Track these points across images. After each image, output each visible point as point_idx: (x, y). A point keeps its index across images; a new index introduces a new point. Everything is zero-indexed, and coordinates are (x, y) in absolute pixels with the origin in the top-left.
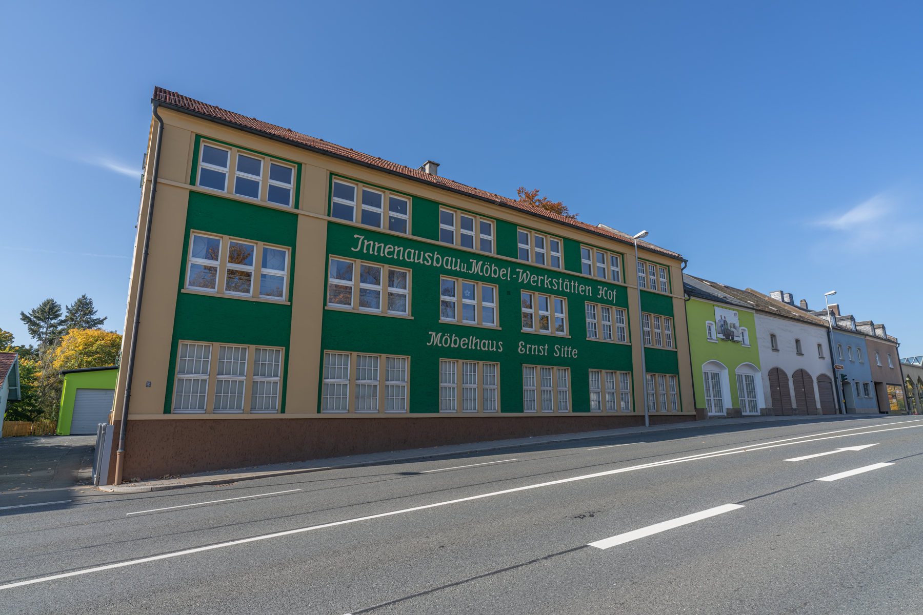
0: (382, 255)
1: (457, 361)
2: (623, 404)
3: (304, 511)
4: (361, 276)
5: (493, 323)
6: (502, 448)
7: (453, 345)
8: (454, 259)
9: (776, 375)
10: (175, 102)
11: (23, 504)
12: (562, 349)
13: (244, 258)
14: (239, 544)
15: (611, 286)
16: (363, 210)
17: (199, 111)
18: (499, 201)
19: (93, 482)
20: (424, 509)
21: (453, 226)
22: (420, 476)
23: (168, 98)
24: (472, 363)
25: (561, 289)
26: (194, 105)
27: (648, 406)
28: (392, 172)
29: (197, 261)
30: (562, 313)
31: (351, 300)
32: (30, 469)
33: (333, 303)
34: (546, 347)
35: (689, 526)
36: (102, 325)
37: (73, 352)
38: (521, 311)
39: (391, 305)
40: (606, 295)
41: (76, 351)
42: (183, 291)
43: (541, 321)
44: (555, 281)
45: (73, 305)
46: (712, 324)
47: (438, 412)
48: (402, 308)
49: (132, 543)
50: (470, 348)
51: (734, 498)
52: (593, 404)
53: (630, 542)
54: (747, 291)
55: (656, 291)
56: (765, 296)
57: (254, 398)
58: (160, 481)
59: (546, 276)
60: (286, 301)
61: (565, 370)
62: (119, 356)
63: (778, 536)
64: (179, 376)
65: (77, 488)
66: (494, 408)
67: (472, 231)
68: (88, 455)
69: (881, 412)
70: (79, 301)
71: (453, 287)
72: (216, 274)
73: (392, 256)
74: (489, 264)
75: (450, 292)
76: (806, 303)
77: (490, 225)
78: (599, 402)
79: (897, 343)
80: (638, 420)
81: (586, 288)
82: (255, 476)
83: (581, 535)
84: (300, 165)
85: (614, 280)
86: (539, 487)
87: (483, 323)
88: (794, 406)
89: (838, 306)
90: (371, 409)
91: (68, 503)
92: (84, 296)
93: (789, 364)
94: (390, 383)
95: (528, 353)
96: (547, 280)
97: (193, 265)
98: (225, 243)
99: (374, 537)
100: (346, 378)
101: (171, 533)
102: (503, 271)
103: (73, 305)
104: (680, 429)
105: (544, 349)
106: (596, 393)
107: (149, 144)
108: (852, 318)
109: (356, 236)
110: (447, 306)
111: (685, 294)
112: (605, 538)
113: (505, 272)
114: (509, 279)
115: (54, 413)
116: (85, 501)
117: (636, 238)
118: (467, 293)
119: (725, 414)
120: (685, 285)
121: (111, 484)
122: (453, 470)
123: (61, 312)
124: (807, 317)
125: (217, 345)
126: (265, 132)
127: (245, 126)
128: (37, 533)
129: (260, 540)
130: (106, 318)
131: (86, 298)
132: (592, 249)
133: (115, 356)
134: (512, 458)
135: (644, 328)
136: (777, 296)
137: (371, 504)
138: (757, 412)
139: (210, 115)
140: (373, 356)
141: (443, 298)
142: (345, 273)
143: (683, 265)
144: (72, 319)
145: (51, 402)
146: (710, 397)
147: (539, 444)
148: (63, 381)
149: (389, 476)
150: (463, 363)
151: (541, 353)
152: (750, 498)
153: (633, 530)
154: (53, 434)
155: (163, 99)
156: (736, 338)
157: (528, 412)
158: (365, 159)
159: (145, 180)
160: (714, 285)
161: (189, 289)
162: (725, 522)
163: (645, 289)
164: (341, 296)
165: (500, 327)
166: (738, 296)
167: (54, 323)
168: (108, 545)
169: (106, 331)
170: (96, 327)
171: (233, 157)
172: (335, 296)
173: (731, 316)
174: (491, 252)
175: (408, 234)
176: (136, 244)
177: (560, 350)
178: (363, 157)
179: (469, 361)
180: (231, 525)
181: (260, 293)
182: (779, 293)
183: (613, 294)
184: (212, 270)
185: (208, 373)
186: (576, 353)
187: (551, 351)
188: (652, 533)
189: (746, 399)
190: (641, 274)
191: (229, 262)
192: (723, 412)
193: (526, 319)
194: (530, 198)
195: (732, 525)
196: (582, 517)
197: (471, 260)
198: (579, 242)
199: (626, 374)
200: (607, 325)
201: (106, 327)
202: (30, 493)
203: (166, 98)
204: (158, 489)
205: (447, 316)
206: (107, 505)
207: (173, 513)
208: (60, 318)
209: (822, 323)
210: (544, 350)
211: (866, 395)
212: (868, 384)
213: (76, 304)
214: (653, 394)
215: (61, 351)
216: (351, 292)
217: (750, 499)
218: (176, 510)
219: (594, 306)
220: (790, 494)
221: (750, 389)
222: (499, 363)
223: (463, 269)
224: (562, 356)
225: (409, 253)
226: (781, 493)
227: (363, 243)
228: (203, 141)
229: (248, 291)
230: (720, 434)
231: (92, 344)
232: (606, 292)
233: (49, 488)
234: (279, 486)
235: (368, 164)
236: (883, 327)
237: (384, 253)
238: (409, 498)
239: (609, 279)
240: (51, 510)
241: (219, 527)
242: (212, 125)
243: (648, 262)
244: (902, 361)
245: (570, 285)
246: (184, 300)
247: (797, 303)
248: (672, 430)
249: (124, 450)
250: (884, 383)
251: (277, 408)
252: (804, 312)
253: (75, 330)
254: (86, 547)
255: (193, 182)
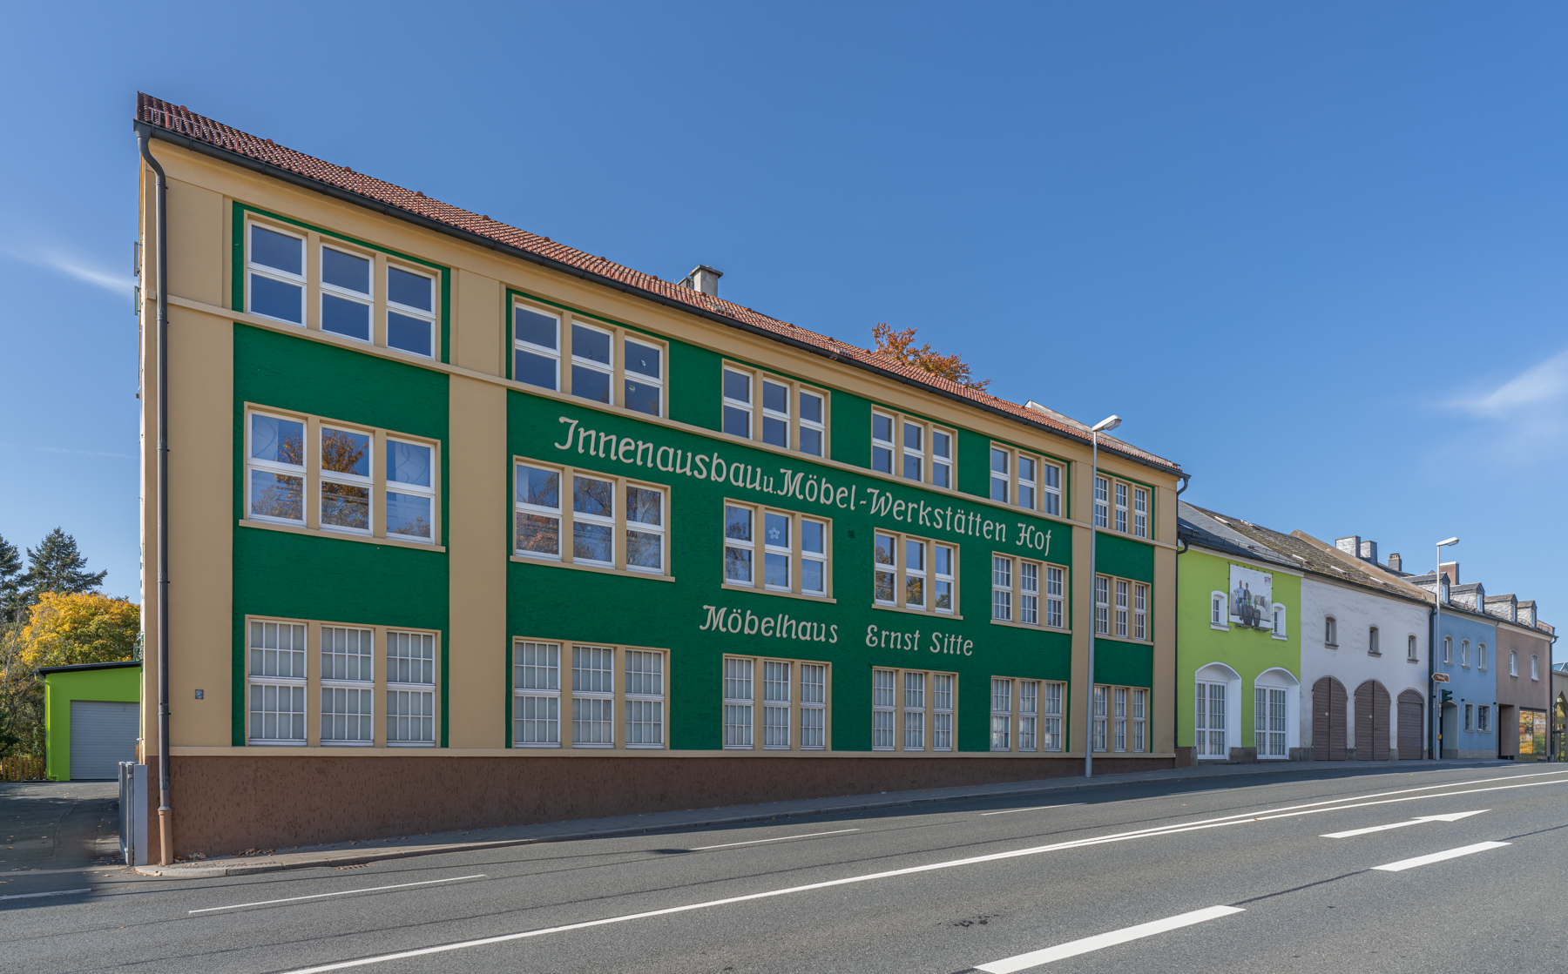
0: (613, 457)
1: (755, 660)
2: (1048, 737)
3: (493, 910)
4: (575, 499)
5: (822, 590)
6: (832, 811)
7: (747, 631)
8: (750, 468)
9: (1327, 692)
10: (184, 128)
11: (8, 895)
12: (946, 640)
13: (351, 462)
14: (387, 961)
15: (1041, 523)
16: (573, 366)
17: (234, 150)
18: (838, 352)
19: (124, 860)
20: (698, 909)
21: (748, 402)
22: (691, 856)
23: (167, 119)
24: (782, 662)
25: (948, 528)
26: (222, 134)
27: (1092, 742)
28: (629, 289)
29: (262, 465)
30: (949, 573)
31: (557, 544)
32: (10, 838)
33: (524, 549)
34: (917, 635)
35: (1148, 941)
36: (99, 586)
37: (54, 635)
38: (873, 569)
39: (632, 555)
40: (1032, 542)
41: (58, 633)
42: (242, 523)
43: (909, 588)
44: (939, 513)
45: (40, 548)
46: (1222, 597)
47: (721, 748)
48: (651, 561)
49: (204, 958)
50: (778, 635)
51: (1229, 896)
52: (995, 738)
53: (1046, 964)
54: (1295, 536)
55: (1125, 535)
56: (1327, 546)
57: (391, 720)
58: (239, 859)
59: (922, 502)
60: (436, 544)
61: (949, 677)
62: (139, 642)
63: (1296, 957)
64: (251, 680)
65: (97, 869)
66: (820, 743)
67: (785, 412)
68: (109, 815)
69: (1501, 757)
70: (49, 539)
71: (747, 522)
72: (301, 491)
73: (632, 460)
74: (815, 477)
75: (742, 532)
76: (1400, 561)
77: (820, 400)
78: (1007, 734)
79: (1552, 636)
80: (1073, 765)
81: (995, 527)
82: (403, 852)
83: (964, 953)
84: (446, 271)
85: (1049, 512)
86: (895, 876)
87: (803, 590)
88: (1351, 744)
89: (1457, 565)
90: (601, 741)
91: (86, 893)
92: (57, 532)
93: (1352, 670)
94: (633, 697)
95: (883, 645)
96: (924, 510)
97: (256, 474)
98: (313, 430)
99: (614, 952)
100: (553, 686)
101: (269, 942)
102: (842, 493)
103: (40, 548)
104: (1146, 782)
105: (912, 640)
106: (1002, 718)
107: (140, 221)
108: (1480, 589)
109: (562, 420)
110: (736, 558)
111: (1179, 541)
112: (1003, 958)
113: (846, 495)
114: (852, 508)
115: (36, 743)
116: (115, 891)
117: (1096, 431)
118: (774, 534)
119: (1226, 757)
120: (1180, 522)
121: (156, 864)
122: (746, 846)
123: (19, 561)
124: (1397, 585)
125: (316, 624)
126: (372, 197)
127: (331, 184)
128: (40, 941)
129: (422, 955)
130: (105, 573)
131: (62, 535)
132: (1012, 451)
133: (131, 644)
134: (850, 828)
135: (1098, 603)
136: (1348, 547)
137: (606, 899)
138: (1284, 754)
139: (256, 158)
140: (602, 648)
141: (730, 542)
142: (545, 492)
143: (1180, 484)
144: (42, 575)
145: (28, 724)
146: (1204, 727)
147: (896, 805)
148: (44, 687)
149: (636, 855)
150: (766, 663)
151: (907, 646)
152: (1256, 896)
153: (1051, 946)
154: (40, 778)
155: (158, 122)
156: (1262, 624)
157: (879, 750)
158: (575, 259)
159: (143, 299)
160: (1234, 524)
161: (255, 519)
162: (1209, 934)
163: (1106, 530)
164: (539, 536)
165: (834, 598)
166: (1276, 545)
167: (11, 581)
168: (164, 961)
169: (109, 598)
170: (88, 589)
171: (311, 251)
172: (528, 536)
173: (1257, 582)
174: (820, 455)
175: (662, 418)
176: (142, 430)
177: (941, 641)
178: (570, 256)
179: (776, 660)
180: (370, 931)
181: (388, 528)
182: (1352, 540)
183: (1046, 539)
184: (293, 483)
185: (305, 675)
186: (971, 646)
187: (925, 642)
188: (1084, 951)
189: (1268, 732)
190: (1100, 502)
191: (323, 468)
192: (1223, 753)
193: (880, 584)
194: (897, 347)
195: (1221, 939)
196: (966, 924)
197: (782, 471)
198: (988, 438)
199: (1059, 685)
200: (1029, 597)
201: (109, 590)
202: (17, 876)
203: (163, 120)
204: (238, 873)
205: (736, 577)
206: (152, 897)
207: (269, 911)
208: (19, 572)
209: (1423, 598)
210: (912, 640)
211: (1480, 727)
212: (1488, 707)
213: (45, 545)
214: (1104, 722)
215: (32, 633)
216: (558, 530)
217: (1254, 899)
218: (274, 907)
219: (1008, 562)
220: (1324, 891)
221: (1280, 716)
222: (830, 663)
223: (768, 487)
224: (945, 651)
225: (665, 454)
226: (1308, 890)
227: (576, 434)
228: (250, 217)
229: (364, 525)
230: (1214, 792)
231: (85, 622)
232: (1033, 534)
233: (49, 869)
234: (447, 870)
235: (582, 270)
236: (1534, 607)
237: (616, 453)
238: (672, 892)
239: (1040, 510)
240: (59, 904)
241: (350, 934)
242: (264, 181)
243: (1115, 478)
244: (1555, 669)
245: (967, 521)
246: (246, 542)
247: (1383, 559)
248: (1131, 783)
249: (170, 807)
250: (1517, 707)
251: (433, 738)
252: (1394, 576)
253: (50, 594)
254: (127, 964)
255: (237, 305)
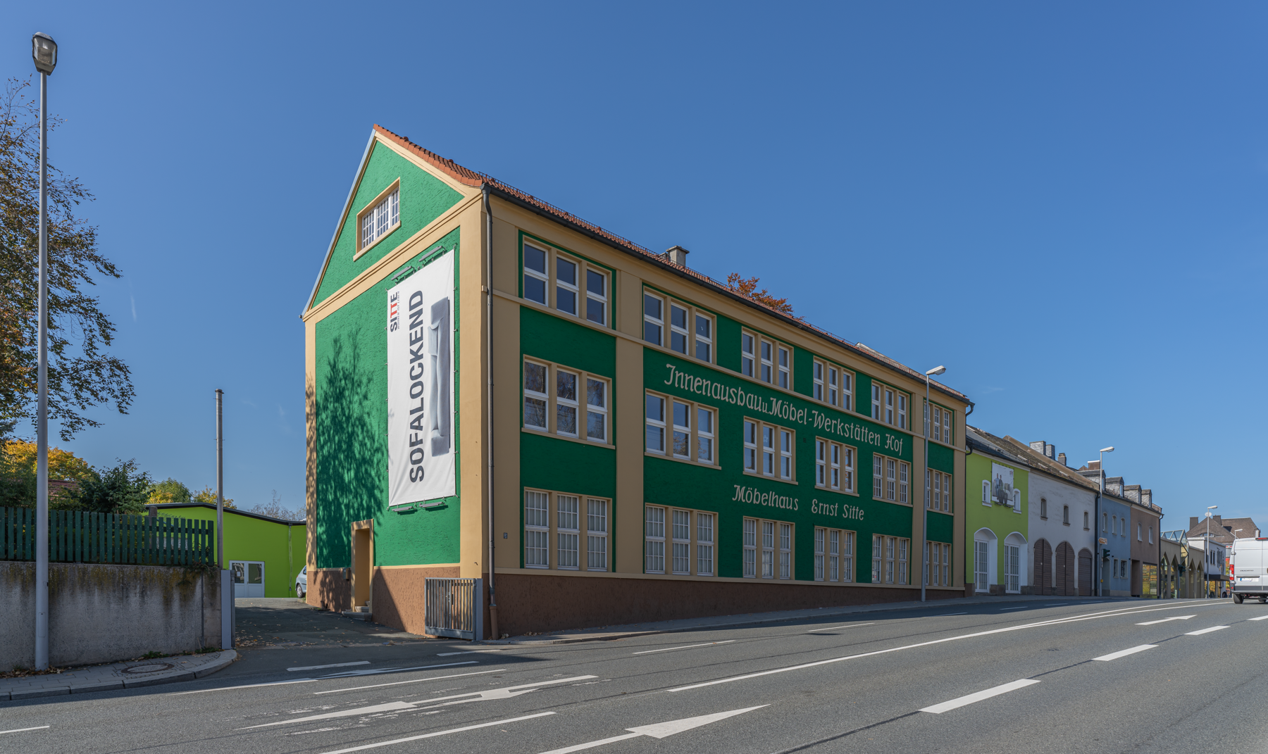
0: (692, 390)
7: (755, 502)
9: (1042, 547)
15: (898, 434)
34: (836, 507)
50: (770, 505)
73: (700, 392)
79: (1160, 514)
80: (914, 594)
84: (614, 271)
88: (1054, 585)
102: (800, 413)
105: (834, 509)
108: (1121, 482)
114: (805, 423)
119: (988, 591)
177: (848, 510)
227: (675, 375)
232: (893, 441)
237: (693, 388)
250: (1141, 562)
